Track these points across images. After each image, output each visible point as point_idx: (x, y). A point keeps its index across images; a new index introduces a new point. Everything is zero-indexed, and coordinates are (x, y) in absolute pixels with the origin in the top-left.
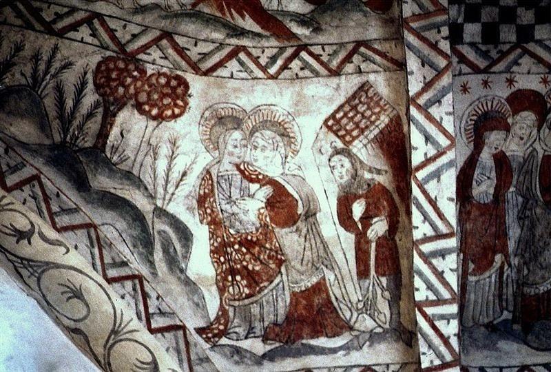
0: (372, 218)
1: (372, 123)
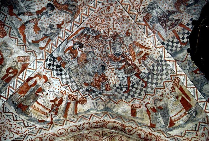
0: (12, 73)
1: (25, 62)
